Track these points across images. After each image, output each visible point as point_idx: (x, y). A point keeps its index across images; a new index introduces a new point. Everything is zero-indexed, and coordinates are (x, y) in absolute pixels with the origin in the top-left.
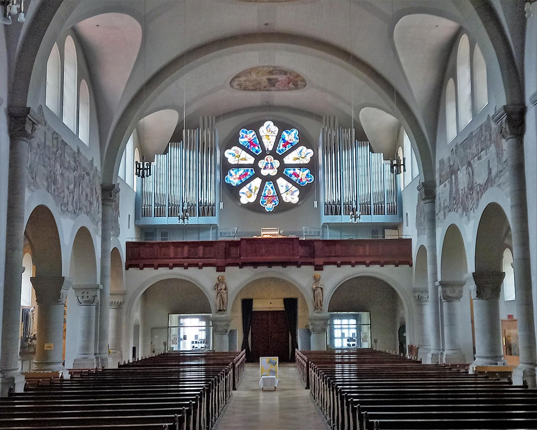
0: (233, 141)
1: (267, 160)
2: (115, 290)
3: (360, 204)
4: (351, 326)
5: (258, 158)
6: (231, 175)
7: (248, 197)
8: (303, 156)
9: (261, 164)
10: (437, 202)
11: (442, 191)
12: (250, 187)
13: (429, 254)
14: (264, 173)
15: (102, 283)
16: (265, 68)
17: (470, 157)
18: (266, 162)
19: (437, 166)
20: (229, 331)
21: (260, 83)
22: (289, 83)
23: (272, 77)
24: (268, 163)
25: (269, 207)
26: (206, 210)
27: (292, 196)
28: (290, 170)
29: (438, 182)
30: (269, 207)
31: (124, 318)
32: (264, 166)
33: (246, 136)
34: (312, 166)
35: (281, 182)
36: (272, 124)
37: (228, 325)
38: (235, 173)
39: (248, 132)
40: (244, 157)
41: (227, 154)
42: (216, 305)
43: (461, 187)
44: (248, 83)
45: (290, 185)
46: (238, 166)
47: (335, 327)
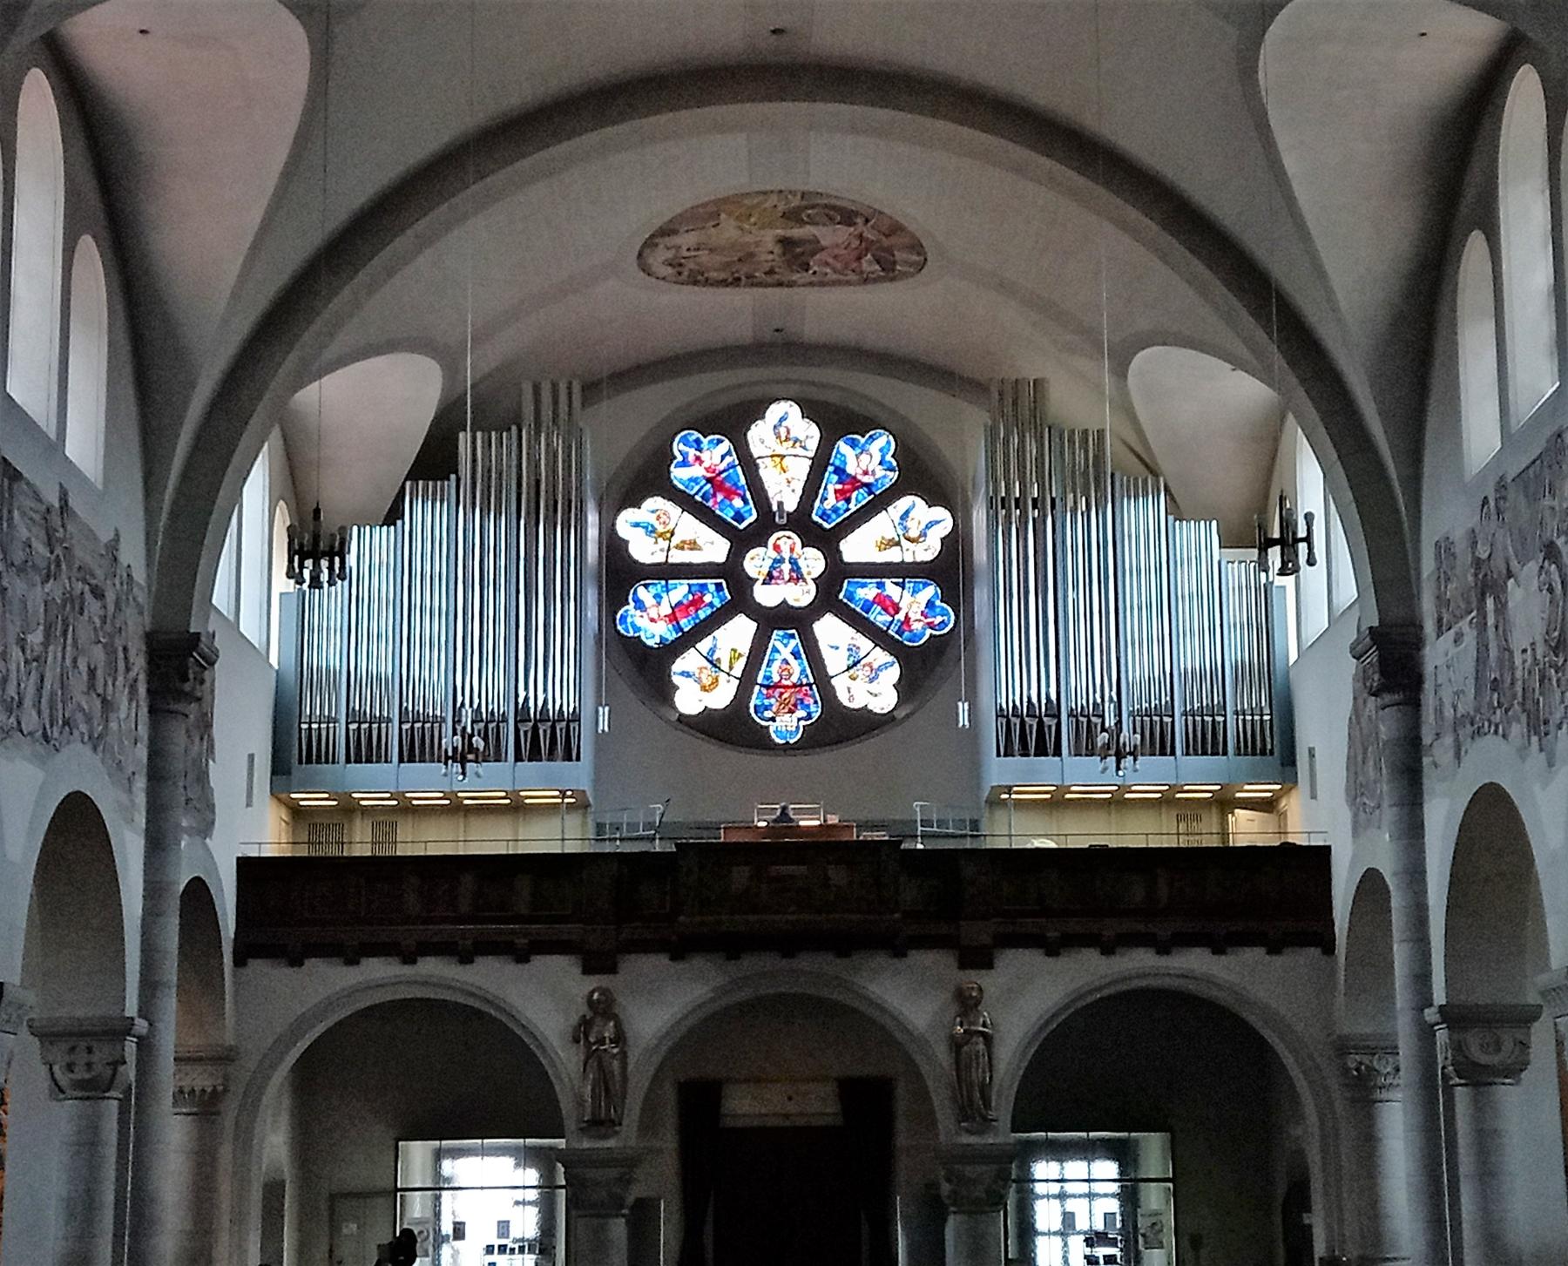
0: (647, 477)
1: (777, 548)
2: (194, 1042)
3: (1131, 714)
4: (1098, 1188)
5: (742, 541)
6: (640, 605)
7: (704, 689)
8: (913, 534)
9: (756, 562)
10: (1429, 699)
11: (1446, 658)
12: (712, 650)
13: (1397, 901)
14: (766, 596)
15: (144, 1012)
16: (774, 199)
17: (1552, 524)
18: (774, 555)
19: (1428, 565)
20: (630, 1200)
21: (751, 255)
22: (859, 258)
23: (797, 232)
24: (781, 561)
25: (786, 726)
26: (545, 737)
27: (872, 688)
28: (864, 586)
29: (1429, 627)
30: (786, 726)
31: (226, 1152)
32: (765, 571)
33: (698, 458)
34: (950, 571)
35: (831, 631)
36: (793, 410)
37: (626, 1181)
38: (657, 596)
39: (705, 441)
41: (625, 523)
42: (580, 1103)
43: (1519, 641)
44: (704, 256)
45: (865, 644)
46: (667, 572)
47: (1040, 1188)
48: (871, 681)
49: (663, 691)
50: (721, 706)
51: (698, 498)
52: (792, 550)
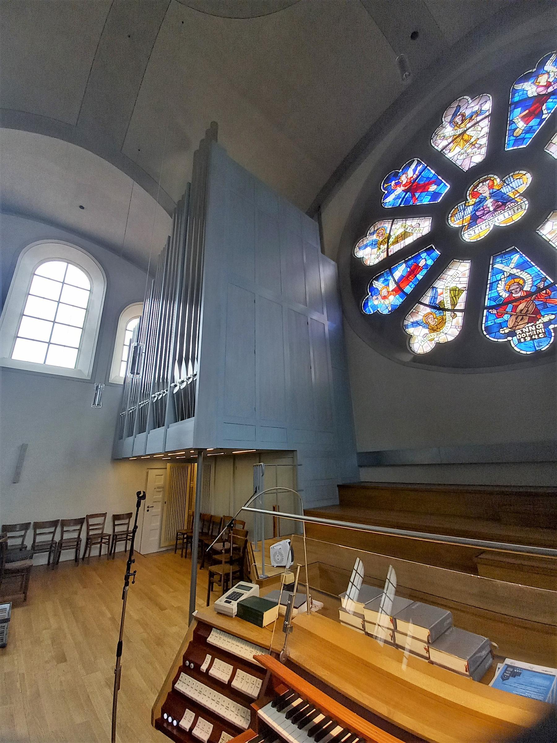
7: (433, 330)
12: (434, 298)
32: (468, 217)
40: (401, 230)
50: (450, 338)
52: (491, 187)
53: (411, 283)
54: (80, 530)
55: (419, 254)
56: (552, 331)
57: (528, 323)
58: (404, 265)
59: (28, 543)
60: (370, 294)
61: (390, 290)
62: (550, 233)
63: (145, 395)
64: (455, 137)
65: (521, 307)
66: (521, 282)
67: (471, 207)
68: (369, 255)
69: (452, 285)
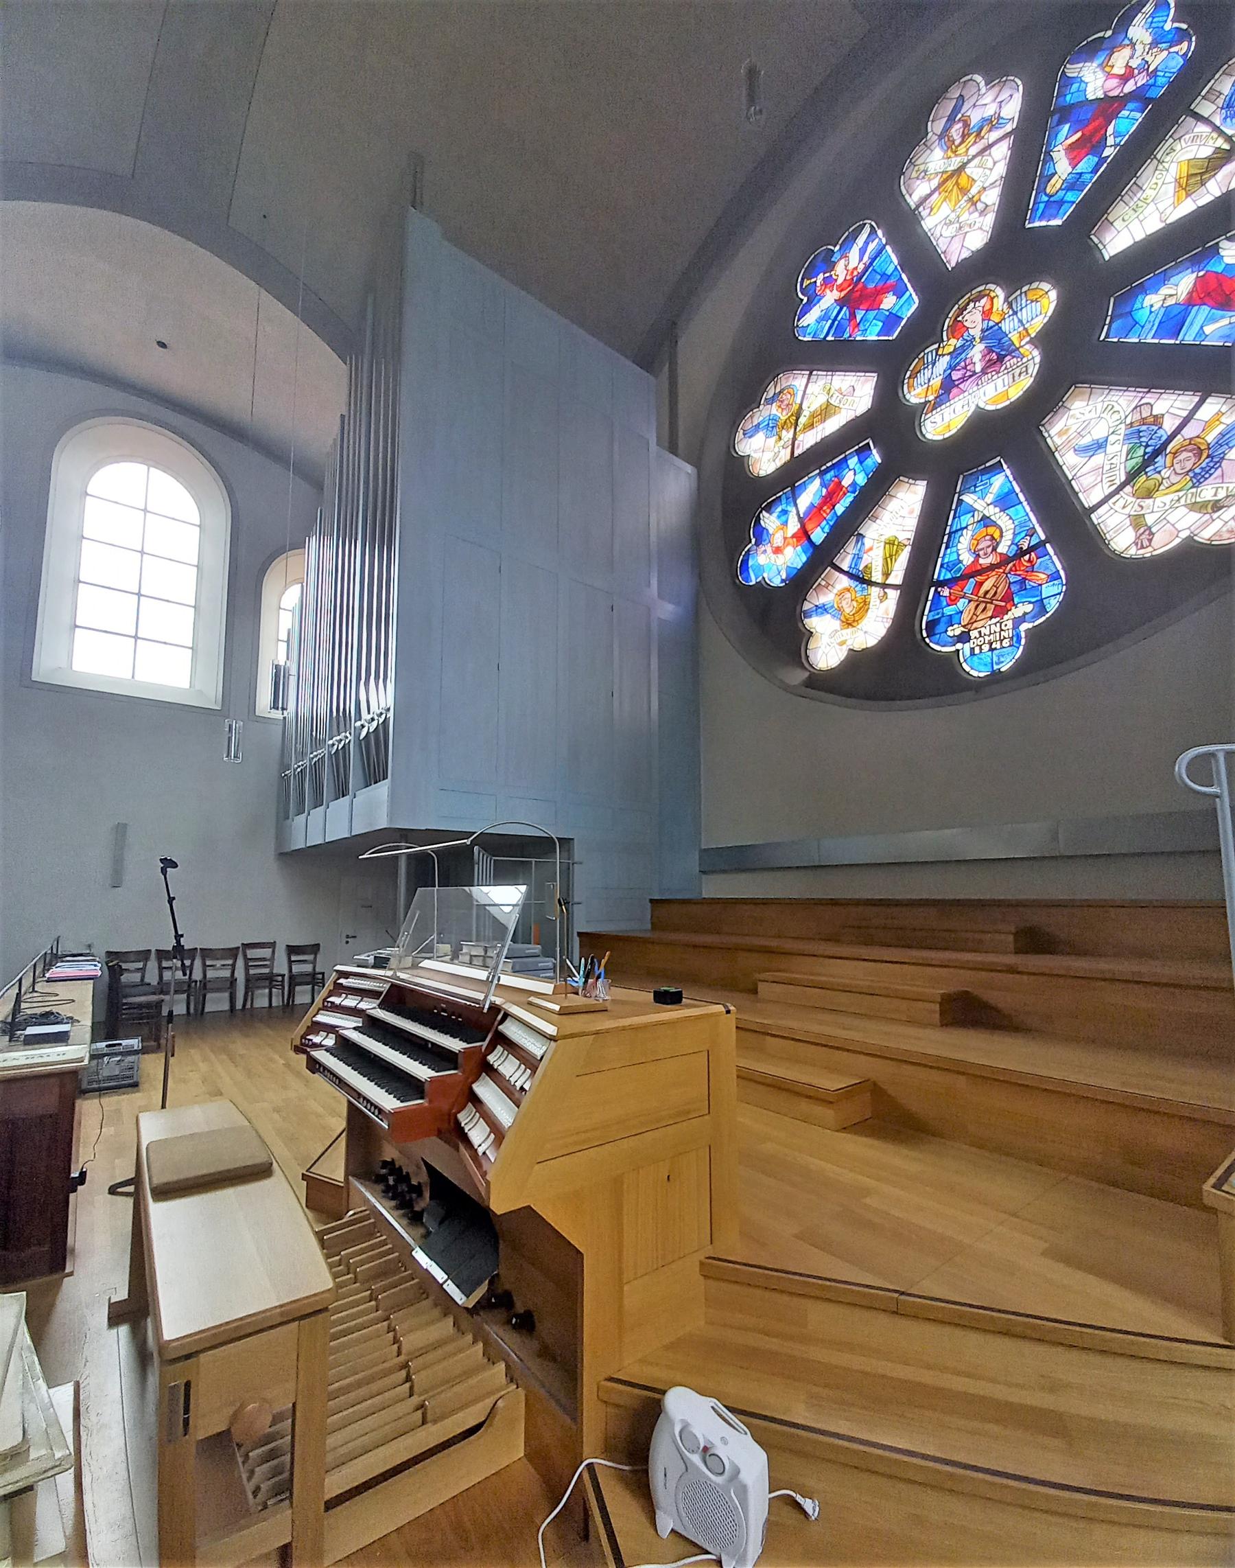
7: (849, 623)
12: (858, 558)
14: (940, 426)
48: (1198, 478)
49: (795, 642)
50: (872, 642)
51: (830, 338)
53: (824, 523)
54: (233, 966)
55: (845, 459)
56: (1023, 635)
57: (991, 618)
58: (817, 481)
59: (152, 978)
60: (753, 541)
61: (789, 534)
62: (1060, 434)
63: (317, 743)
64: (945, 176)
65: (987, 585)
66: (997, 535)
67: (947, 358)
68: (763, 452)
69: (889, 534)
